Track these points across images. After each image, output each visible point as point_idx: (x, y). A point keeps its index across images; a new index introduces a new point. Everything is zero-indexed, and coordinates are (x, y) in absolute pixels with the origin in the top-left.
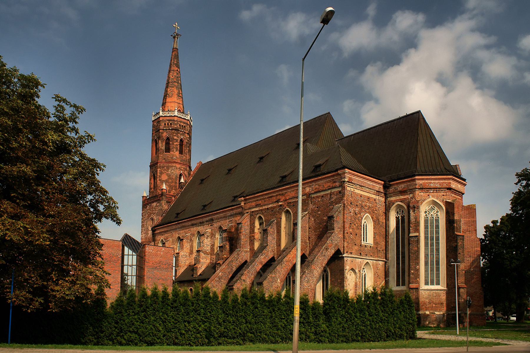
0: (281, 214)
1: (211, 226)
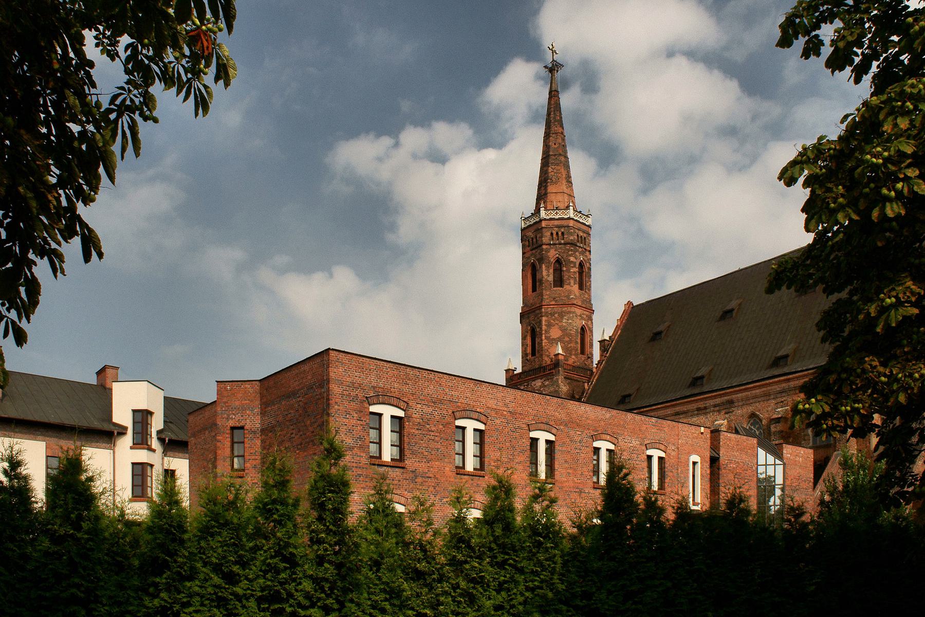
1: (726, 413)
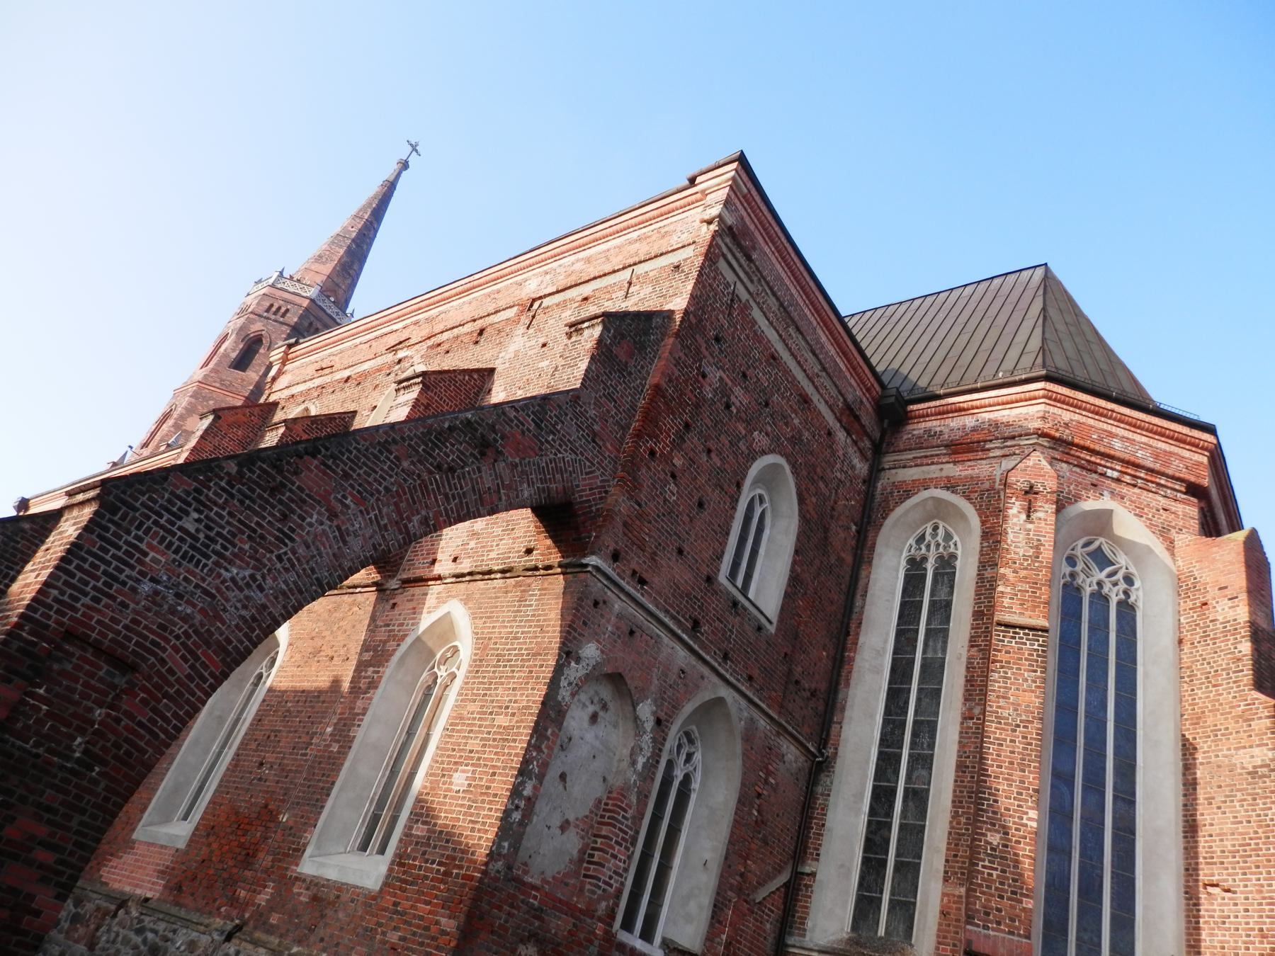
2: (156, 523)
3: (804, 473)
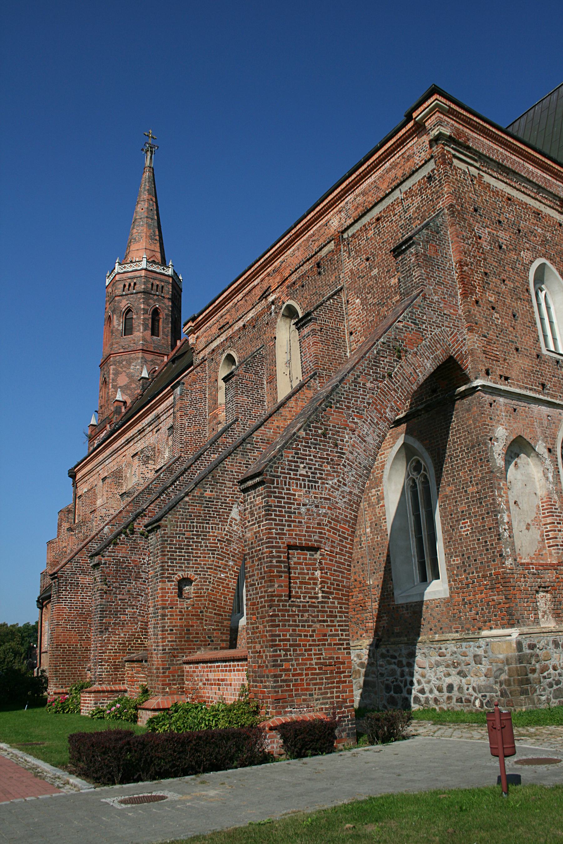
0: (271, 324)
2: (290, 478)
3: (558, 259)
